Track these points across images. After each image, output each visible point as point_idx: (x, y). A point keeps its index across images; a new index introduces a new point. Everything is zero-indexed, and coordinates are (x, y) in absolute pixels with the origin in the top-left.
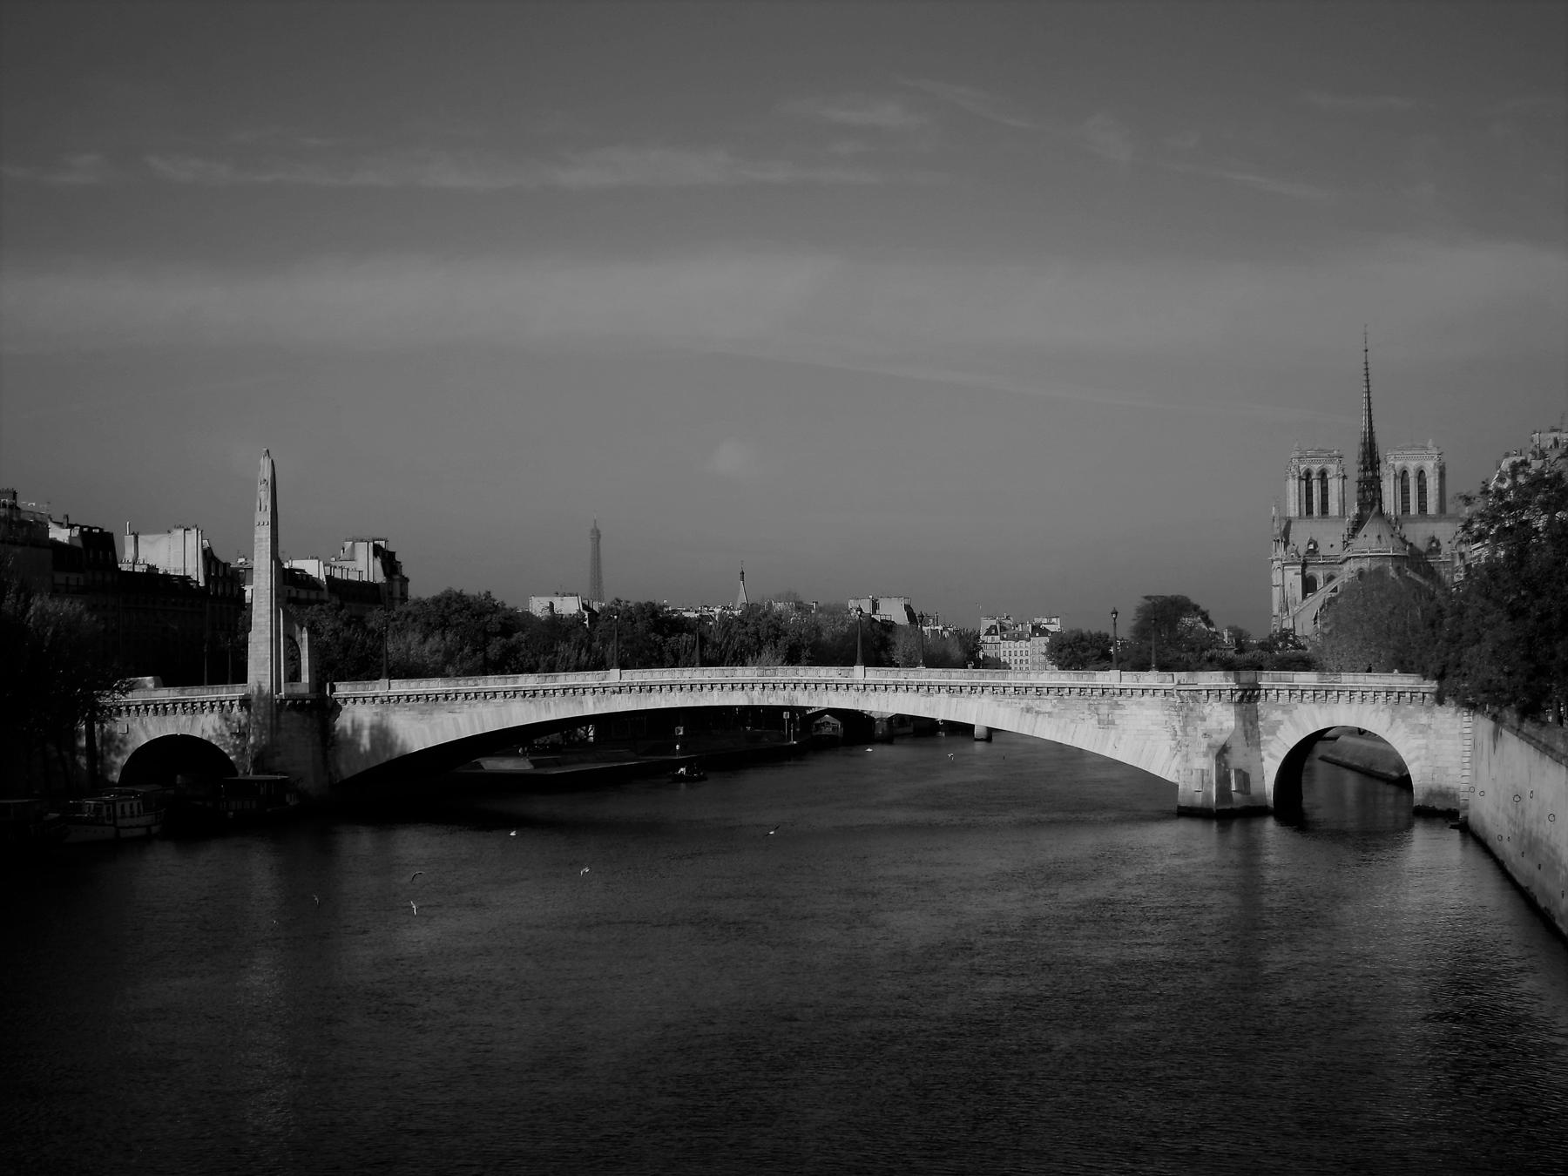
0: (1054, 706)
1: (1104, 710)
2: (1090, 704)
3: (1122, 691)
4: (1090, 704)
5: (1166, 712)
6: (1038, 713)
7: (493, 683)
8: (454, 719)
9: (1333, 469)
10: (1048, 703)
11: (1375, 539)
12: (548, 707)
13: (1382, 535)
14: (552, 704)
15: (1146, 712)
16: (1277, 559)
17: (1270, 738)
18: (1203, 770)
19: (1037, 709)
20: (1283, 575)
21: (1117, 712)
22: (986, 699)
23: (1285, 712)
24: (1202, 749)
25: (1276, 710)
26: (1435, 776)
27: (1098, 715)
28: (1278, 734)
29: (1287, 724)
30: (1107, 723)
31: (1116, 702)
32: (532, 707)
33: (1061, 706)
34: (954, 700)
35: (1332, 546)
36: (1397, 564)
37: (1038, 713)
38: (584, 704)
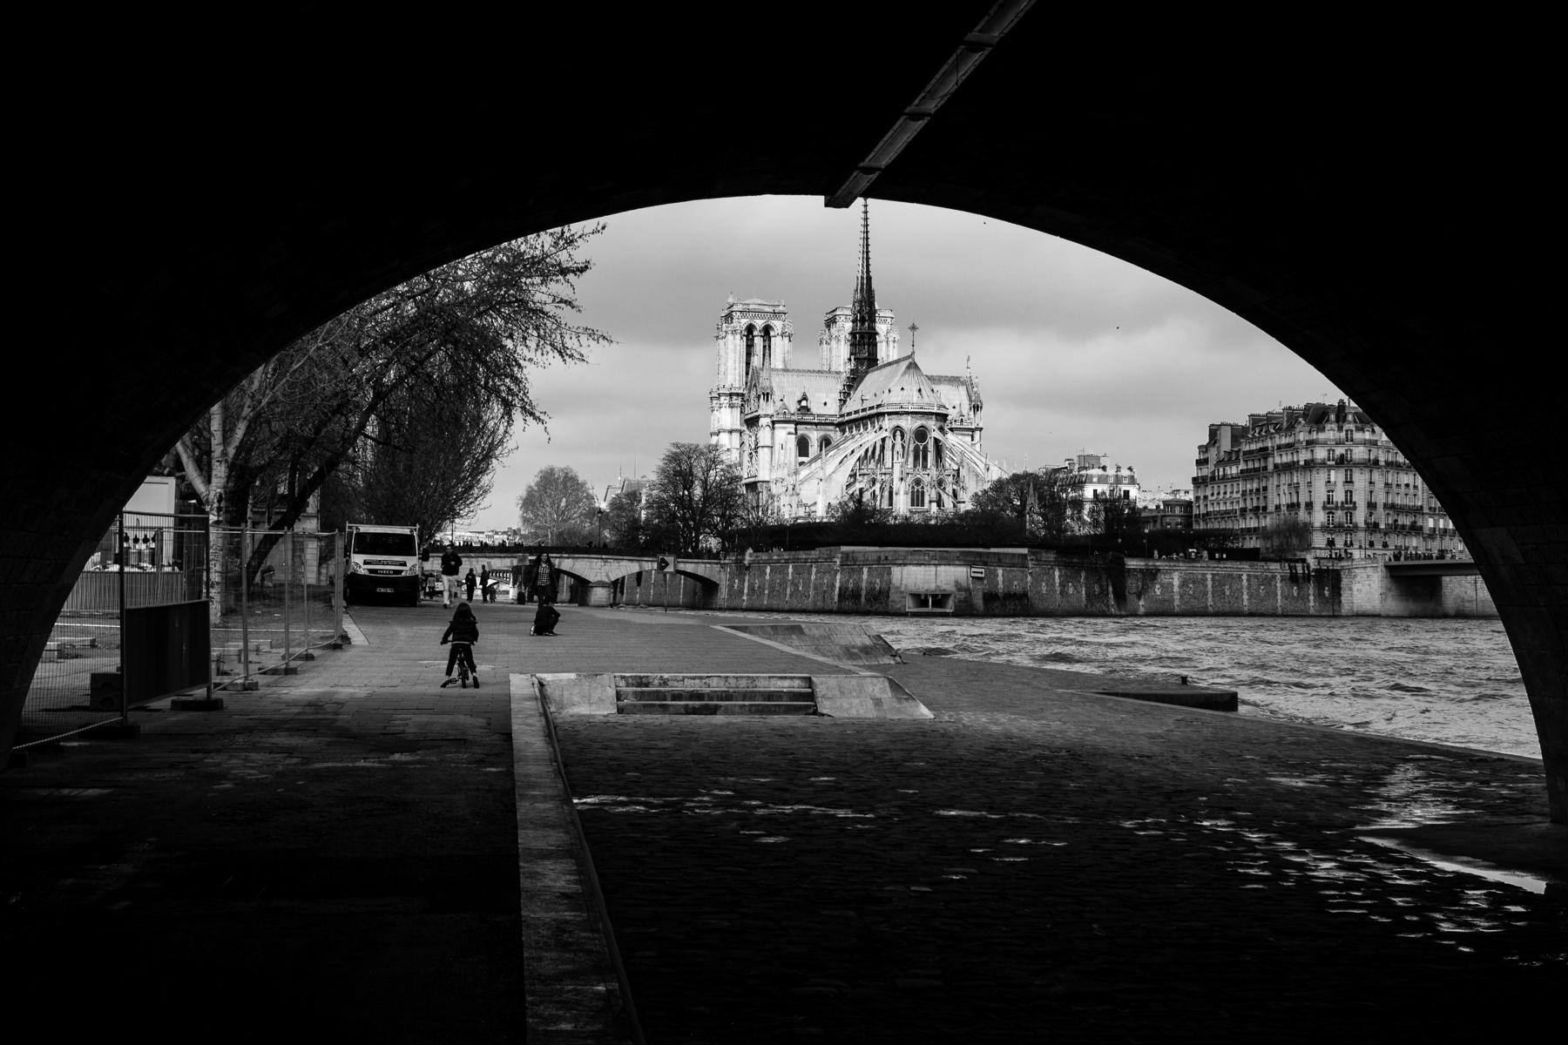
9: (777, 325)
11: (916, 394)
13: (922, 388)
16: (766, 416)
20: (773, 434)
35: (825, 404)
36: (939, 424)
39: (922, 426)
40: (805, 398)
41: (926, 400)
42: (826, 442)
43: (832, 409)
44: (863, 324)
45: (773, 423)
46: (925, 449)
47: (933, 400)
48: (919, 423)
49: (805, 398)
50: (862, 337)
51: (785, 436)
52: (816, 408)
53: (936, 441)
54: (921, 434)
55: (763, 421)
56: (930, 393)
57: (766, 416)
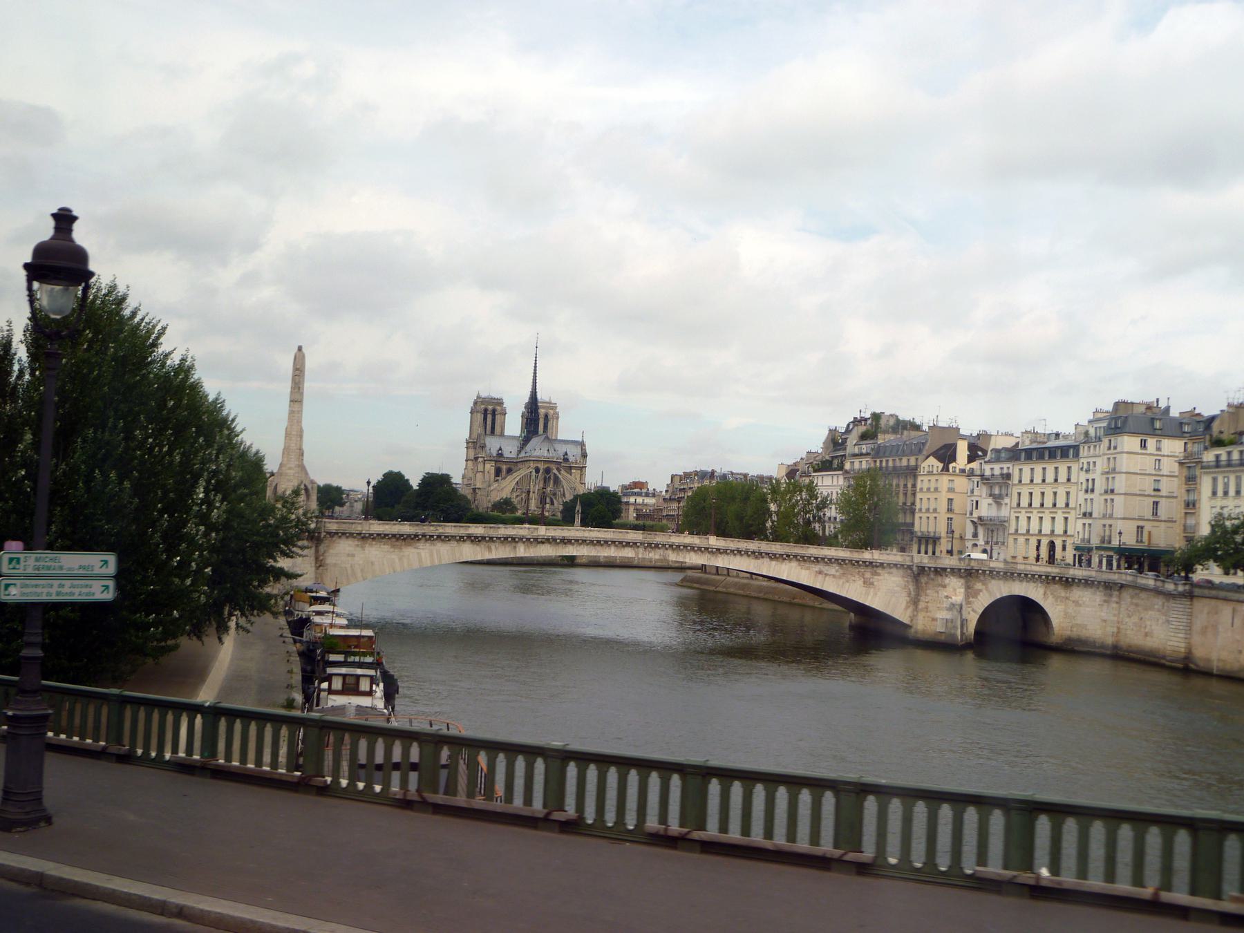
0: (837, 571)
1: (868, 575)
2: (859, 572)
3: (882, 564)
4: (859, 572)
5: (906, 579)
6: (826, 575)
7: (450, 529)
8: (418, 553)
10: (833, 570)
11: (546, 452)
12: (490, 549)
14: (493, 547)
15: (894, 579)
16: (481, 457)
17: (974, 599)
18: (947, 619)
19: (826, 572)
21: (876, 577)
22: (794, 564)
23: (983, 584)
24: (945, 605)
25: (979, 582)
26: (1075, 629)
27: (864, 578)
28: (979, 597)
29: (984, 591)
30: (868, 584)
31: (875, 572)
32: (478, 548)
33: (841, 571)
34: (774, 563)
37: (826, 575)
38: (517, 549)
39: (548, 467)
40: (500, 449)
41: (551, 455)
42: (509, 471)
43: (514, 455)
44: (531, 414)
45: (485, 460)
46: (549, 477)
47: (554, 455)
48: (546, 466)
49: (500, 449)
50: (531, 420)
51: (490, 467)
52: (506, 454)
53: (555, 474)
54: (548, 471)
55: (480, 460)
56: (553, 452)
57: (481, 457)
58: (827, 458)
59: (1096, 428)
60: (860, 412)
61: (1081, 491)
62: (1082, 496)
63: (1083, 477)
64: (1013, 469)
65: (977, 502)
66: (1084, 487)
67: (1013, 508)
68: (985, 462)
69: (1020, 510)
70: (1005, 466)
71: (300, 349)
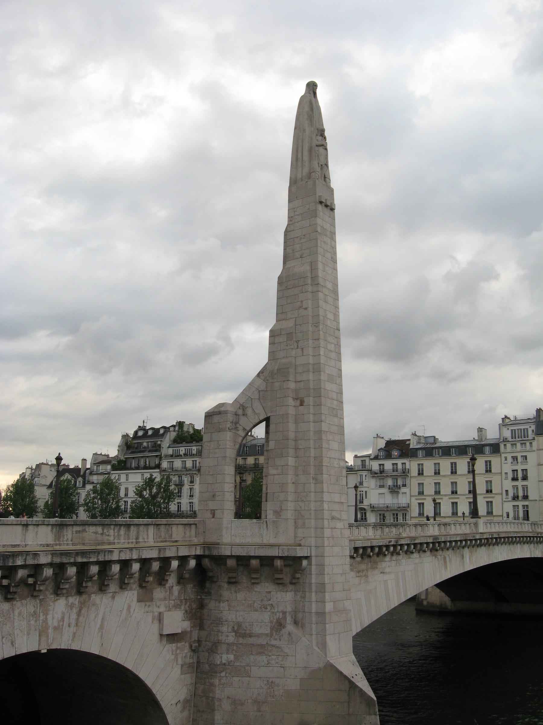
58: (122, 458)
59: (512, 430)
60: (144, 422)
61: (506, 478)
62: (508, 485)
63: (508, 468)
64: (412, 465)
65: (366, 492)
66: (510, 476)
67: (413, 496)
68: (371, 459)
69: (458, 497)
70: (399, 462)
71: (312, 87)
